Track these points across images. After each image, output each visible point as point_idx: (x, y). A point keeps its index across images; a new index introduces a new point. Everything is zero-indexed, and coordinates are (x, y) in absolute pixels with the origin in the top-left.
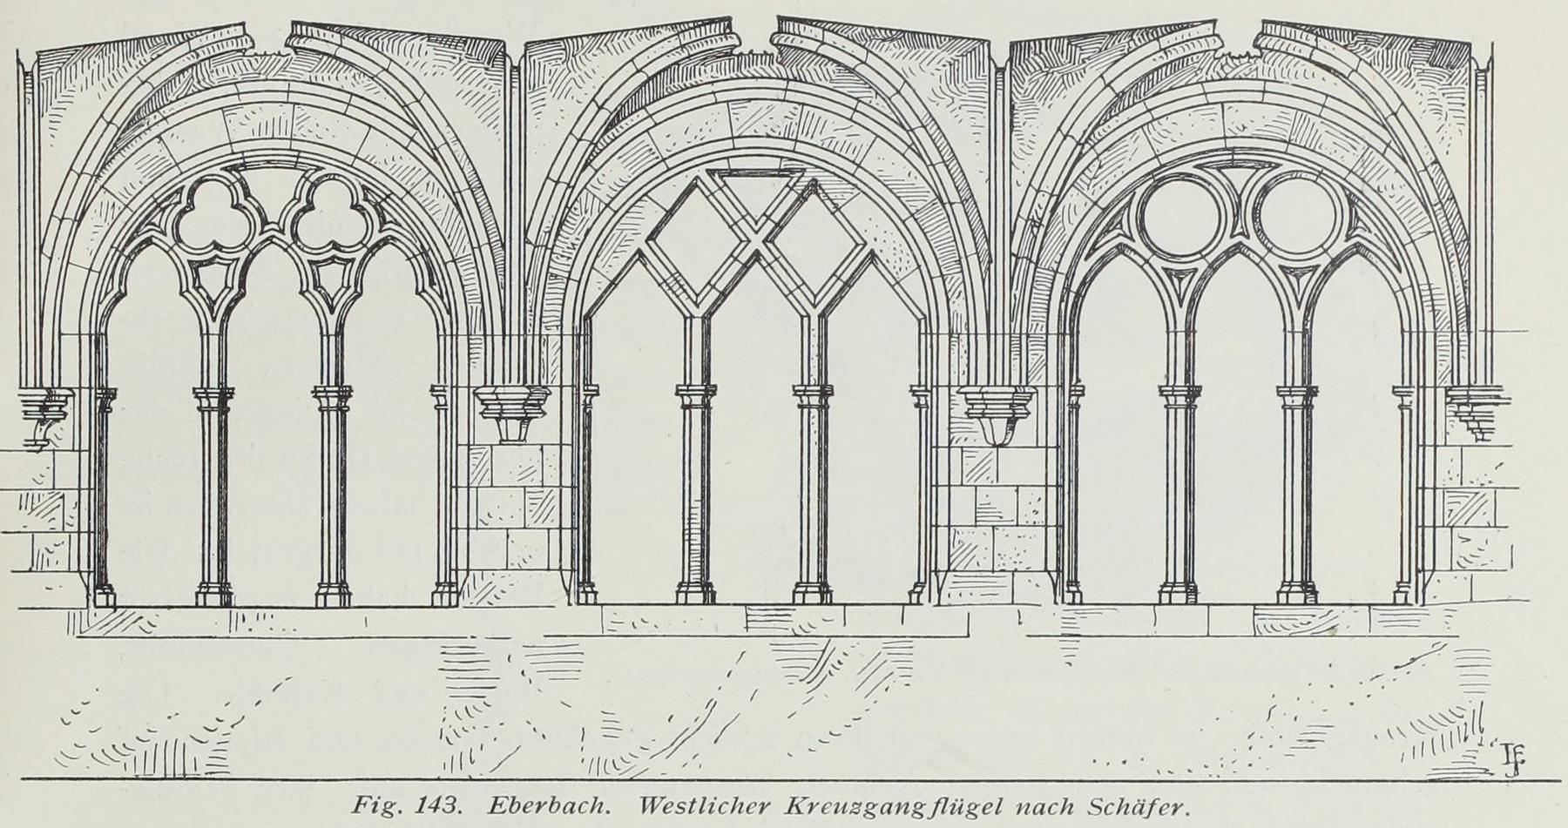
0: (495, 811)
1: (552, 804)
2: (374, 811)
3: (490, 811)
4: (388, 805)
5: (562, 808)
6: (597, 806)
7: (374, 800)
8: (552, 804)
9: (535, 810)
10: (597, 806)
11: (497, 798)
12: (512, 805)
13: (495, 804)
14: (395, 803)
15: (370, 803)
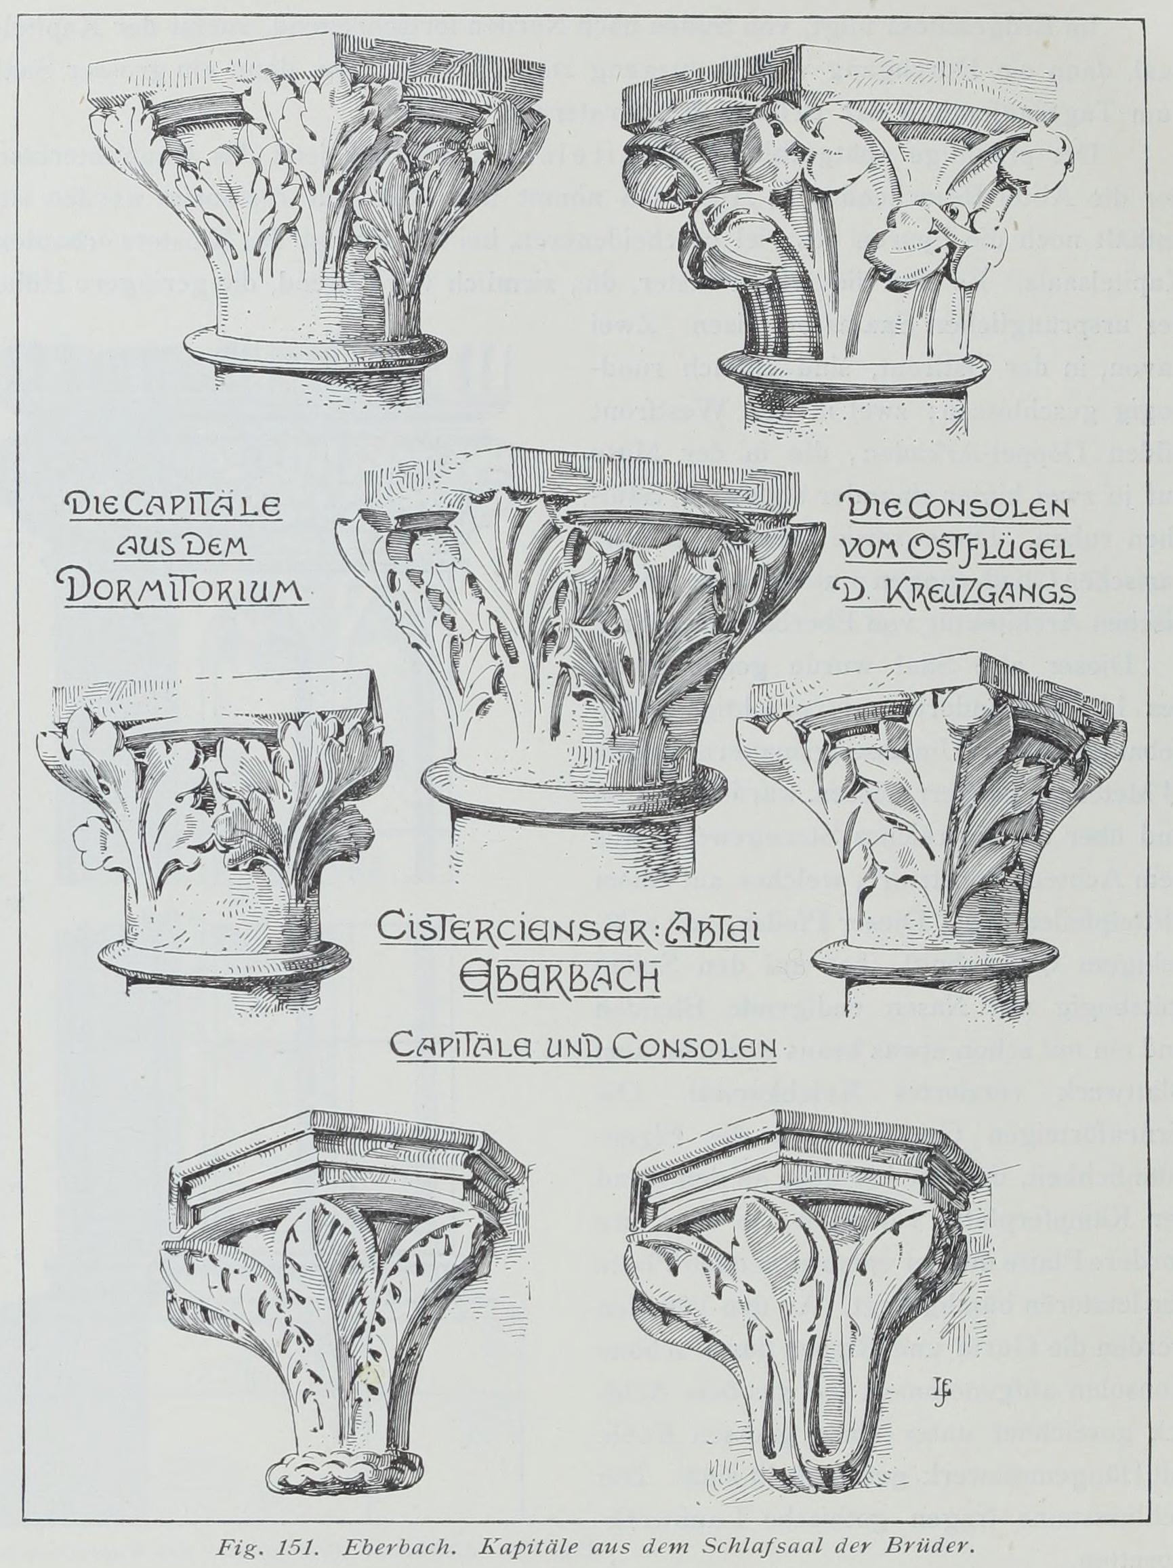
0: (349, 1552)
1: (402, 1546)
2: (237, 1553)
3: (218, 1552)
4: (250, 1547)
5: (410, 1550)
6: (443, 1548)
7: (237, 1543)
8: (402, 1546)
9: (387, 1552)
10: (443, 1548)
11: (351, 1541)
12: (365, 1547)
13: (223, 1546)
14: (256, 1546)
15: (233, 1545)
